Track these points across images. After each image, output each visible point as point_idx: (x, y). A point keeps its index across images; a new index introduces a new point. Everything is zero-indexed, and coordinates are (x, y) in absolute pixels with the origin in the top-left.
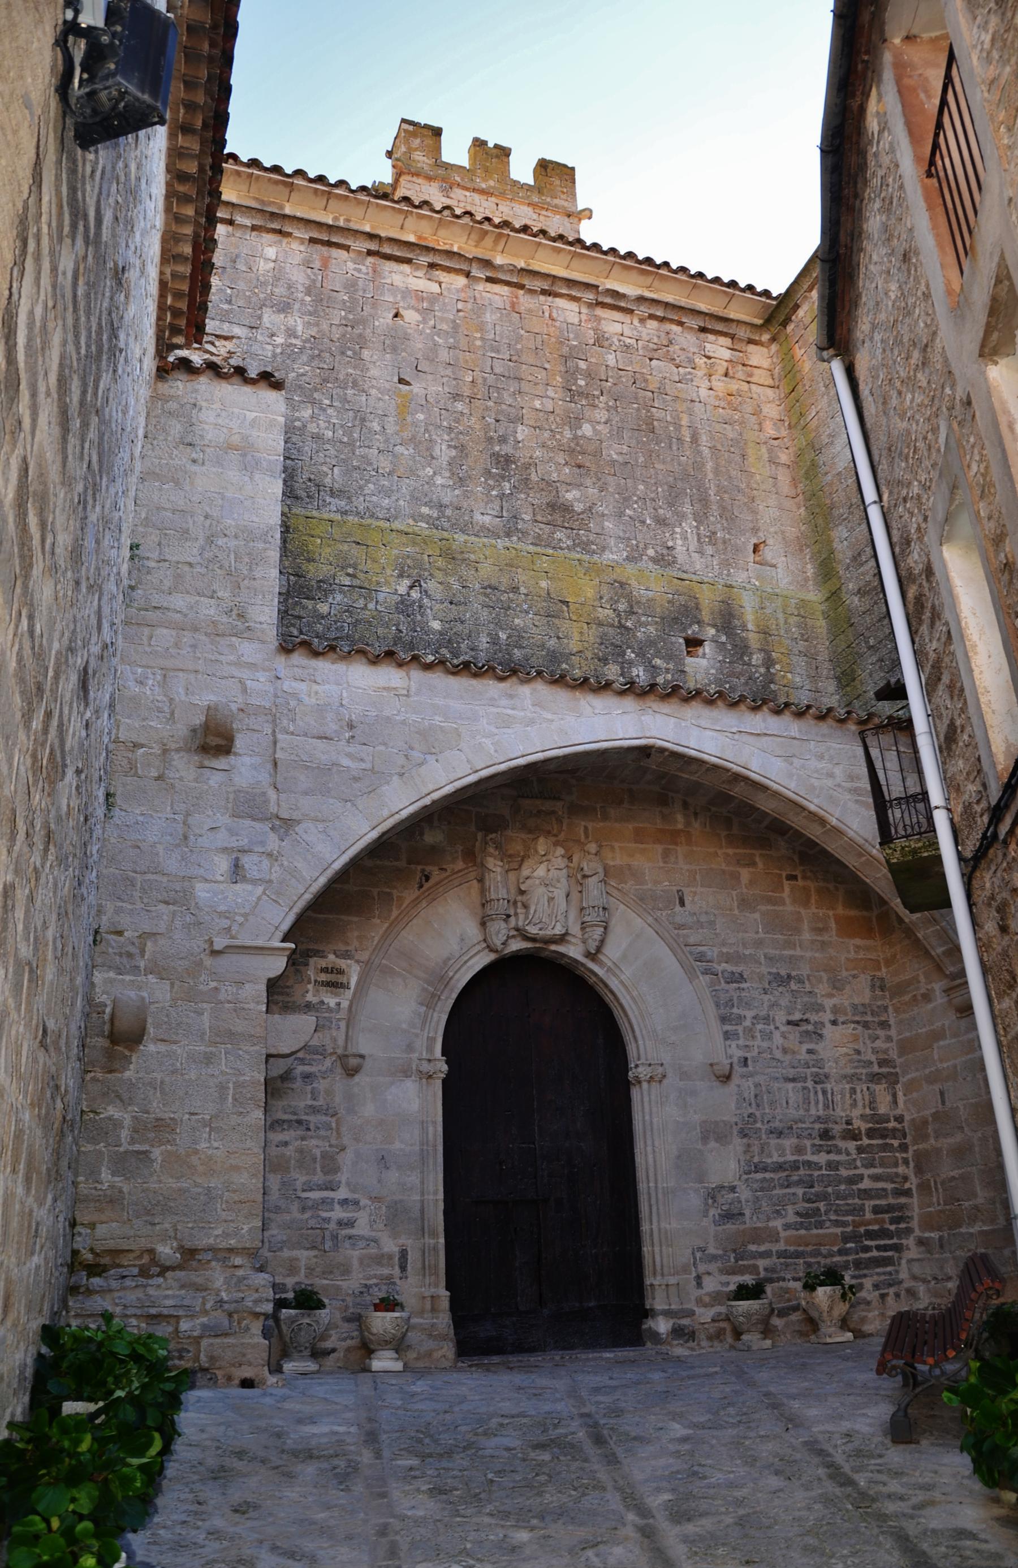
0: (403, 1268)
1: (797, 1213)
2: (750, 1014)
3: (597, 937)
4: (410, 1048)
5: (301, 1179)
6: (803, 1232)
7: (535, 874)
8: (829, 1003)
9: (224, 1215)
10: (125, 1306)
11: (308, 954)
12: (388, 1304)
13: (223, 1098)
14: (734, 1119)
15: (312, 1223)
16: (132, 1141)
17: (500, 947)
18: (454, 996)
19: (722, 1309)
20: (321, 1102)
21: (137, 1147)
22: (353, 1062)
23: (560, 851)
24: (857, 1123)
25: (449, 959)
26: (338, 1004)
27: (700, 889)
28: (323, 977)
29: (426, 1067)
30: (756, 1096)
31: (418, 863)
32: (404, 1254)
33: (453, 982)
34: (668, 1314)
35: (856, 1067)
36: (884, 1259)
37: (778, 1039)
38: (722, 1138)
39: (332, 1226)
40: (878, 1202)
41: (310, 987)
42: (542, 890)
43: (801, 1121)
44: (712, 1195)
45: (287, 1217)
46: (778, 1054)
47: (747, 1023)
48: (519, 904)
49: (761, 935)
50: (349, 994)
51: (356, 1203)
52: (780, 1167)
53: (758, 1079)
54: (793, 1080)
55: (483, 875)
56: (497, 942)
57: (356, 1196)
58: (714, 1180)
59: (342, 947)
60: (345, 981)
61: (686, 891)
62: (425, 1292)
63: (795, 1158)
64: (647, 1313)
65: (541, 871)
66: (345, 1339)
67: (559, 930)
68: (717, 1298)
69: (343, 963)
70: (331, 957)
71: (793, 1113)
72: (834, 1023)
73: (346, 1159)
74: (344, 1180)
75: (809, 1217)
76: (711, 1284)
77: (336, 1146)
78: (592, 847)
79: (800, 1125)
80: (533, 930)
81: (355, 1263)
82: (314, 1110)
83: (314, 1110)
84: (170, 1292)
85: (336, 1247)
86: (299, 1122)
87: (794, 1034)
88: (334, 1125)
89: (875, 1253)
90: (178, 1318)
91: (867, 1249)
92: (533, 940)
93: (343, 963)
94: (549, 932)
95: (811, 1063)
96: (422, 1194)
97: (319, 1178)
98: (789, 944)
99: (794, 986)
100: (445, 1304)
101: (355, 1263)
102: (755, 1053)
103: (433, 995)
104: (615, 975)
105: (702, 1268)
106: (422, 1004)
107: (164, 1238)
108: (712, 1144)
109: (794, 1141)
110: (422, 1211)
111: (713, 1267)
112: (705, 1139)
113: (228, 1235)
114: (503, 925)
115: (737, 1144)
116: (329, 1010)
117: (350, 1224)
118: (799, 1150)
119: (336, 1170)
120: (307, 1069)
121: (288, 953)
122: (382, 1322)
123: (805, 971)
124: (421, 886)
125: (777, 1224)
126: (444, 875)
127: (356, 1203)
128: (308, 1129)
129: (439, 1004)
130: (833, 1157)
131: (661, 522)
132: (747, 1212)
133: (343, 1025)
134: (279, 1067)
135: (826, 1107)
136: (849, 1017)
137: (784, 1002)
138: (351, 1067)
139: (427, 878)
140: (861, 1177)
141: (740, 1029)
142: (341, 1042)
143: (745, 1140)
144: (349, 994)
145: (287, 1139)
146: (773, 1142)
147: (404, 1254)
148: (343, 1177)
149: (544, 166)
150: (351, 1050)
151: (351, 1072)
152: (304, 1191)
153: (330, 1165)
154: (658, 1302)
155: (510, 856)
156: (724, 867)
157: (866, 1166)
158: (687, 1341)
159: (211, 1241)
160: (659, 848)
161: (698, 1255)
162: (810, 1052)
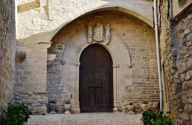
0: (71, 97)
1: (142, 91)
2: (135, 56)
3: (108, 41)
4: (74, 60)
5: (54, 82)
6: (142, 95)
8: (151, 55)
9: (40, 87)
10: (23, 102)
11: (55, 43)
12: (68, 103)
13: (40, 68)
14: (131, 74)
15: (56, 90)
16: (24, 75)
17: (90, 43)
18: (82, 51)
19: (126, 107)
20: (58, 69)
21: (25, 76)
22: (63, 62)
23: (102, 25)
24: (154, 76)
26: (61, 52)
27: (128, 33)
28: (58, 47)
29: (76, 64)
30: (136, 70)
32: (72, 95)
33: (82, 49)
34: (117, 107)
35: (155, 66)
36: (157, 100)
37: (141, 61)
38: (129, 78)
39: (59, 90)
40: (157, 90)
41: (56, 49)
43: (144, 75)
44: (126, 87)
45: (52, 89)
46: (141, 64)
47: (135, 58)
48: (94, 35)
49: (139, 42)
50: (63, 50)
51: (64, 86)
52: (139, 83)
53: (136, 68)
54: (143, 68)
57: (64, 85)
58: (127, 85)
59: (62, 42)
60: (62, 48)
61: (125, 33)
62: (75, 103)
63: (142, 82)
64: (114, 107)
65: (98, 29)
66: (61, 109)
67: (101, 40)
68: (126, 105)
69: (62, 45)
70: (60, 44)
71: (142, 74)
72: (152, 58)
73: (63, 78)
74: (62, 82)
75: (144, 93)
76: (125, 103)
77: (60, 77)
78: (108, 25)
79: (143, 76)
80: (96, 40)
81: (63, 97)
82: (57, 70)
83: (57, 70)
84: (30, 100)
85: (60, 94)
86: (54, 72)
87: (144, 60)
88: (60, 73)
89: (156, 99)
90: (32, 104)
91: (154, 98)
92: (96, 42)
93: (62, 45)
94: (99, 40)
95: (147, 65)
96: (75, 85)
97: (57, 82)
98: (144, 44)
99: (144, 51)
100: (79, 104)
101: (63, 97)
102: (136, 63)
103: (78, 51)
105: (124, 100)
106: (76, 53)
107: (30, 91)
108: (127, 79)
109: (142, 79)
110: (75, 88)
111: (126, 100)
112: (126, 78)
113: (41, 91)
114: (91, 39)
115: (132, 79)
116: (59, 53)
117: (63, 90)
118: (143, 80)
119: (60, 81)
120: (55, 63)
121: (51, 44)
122: (67, 106)
123: (147, 48)
124: (76, 31)
125: (138, 93)
126: (80, 29)
127: (64, 86)
128: (56, 74)
129: (79, 53)
130: (149, 82)
132: (133, 91)
133: (62, 56)
134: (50, 63)
135: (149, 73)
136: (155, 57)
137: (142, 54)
138: (63, 63)
139: (77, 30)
140: (154, 86)
141: (134, 59)
142: (61, 59)
143: (133, 78)
144: (63, 50)
145: (52, 75)
146: (138, 79)
147: (72, 95)
148: (61, 82)
150: (63, 60)
151: (63, 64)
152: (55, 84)
153: (59, 80)
154: (115, 105)
156: (133, 29)
157: (155, 84)
158: (120, 112)
159: (38, 91)
160: (121, 25)
161: (123, 98)
162: (146, 63)
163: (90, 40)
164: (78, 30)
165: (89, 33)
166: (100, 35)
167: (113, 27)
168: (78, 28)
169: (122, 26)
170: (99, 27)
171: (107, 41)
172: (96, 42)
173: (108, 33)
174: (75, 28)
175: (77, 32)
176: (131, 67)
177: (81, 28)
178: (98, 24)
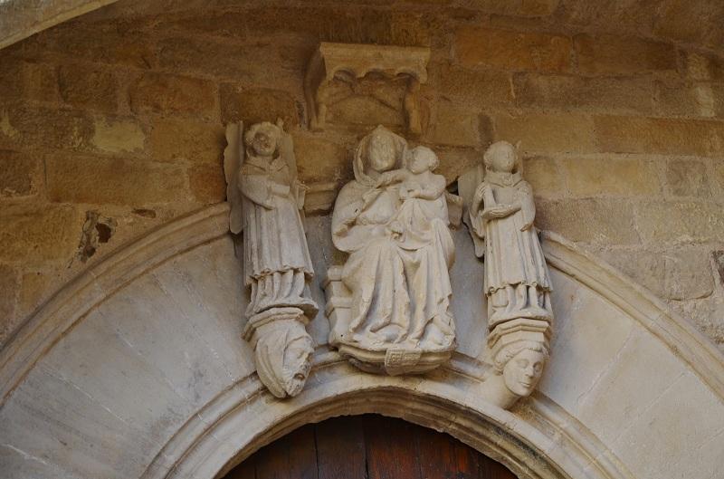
3: (533, 357)
7: (370, 214)
17: (292, 386)
23: (425, 157)
25: (166, 422)
31: (79, 199)
42: (388, 245)
48: (335, 288)
55: (243, 220)
56: (286, 371)
65: (382, 208)
67: (436, 341)
78: (502, 153)
80: (371, 342)
92: (376, 369)
94: (410, 347)
104: (580, 449)
114: (298, 330)
124: (91, 252)
126: (148, 222)
139: (105, 233)
155: (309, 181)
160: (660, 162)
164: (117, 239)
165: (271, 264)
166: (419, 279)
167: (566, 187)
168: (106, 213)
169: (678, 175)
170: (389, 176)
171: (523, 350)
172: (376, 369)
173: (511, 253)
174: (66, 206)
175: (106, 258)
177: (152, 213)
178: (369, 144)
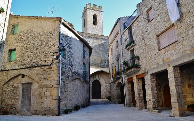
131: (104, 54)
149: (99, 6)
163: (94, 79)
167: (101, 75)
171: (99, 79)
173: (99, 77)
176: (106, 86)
